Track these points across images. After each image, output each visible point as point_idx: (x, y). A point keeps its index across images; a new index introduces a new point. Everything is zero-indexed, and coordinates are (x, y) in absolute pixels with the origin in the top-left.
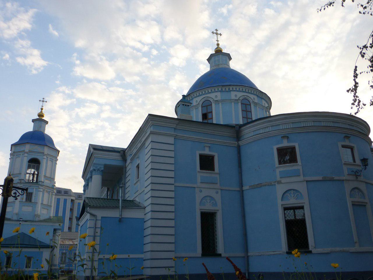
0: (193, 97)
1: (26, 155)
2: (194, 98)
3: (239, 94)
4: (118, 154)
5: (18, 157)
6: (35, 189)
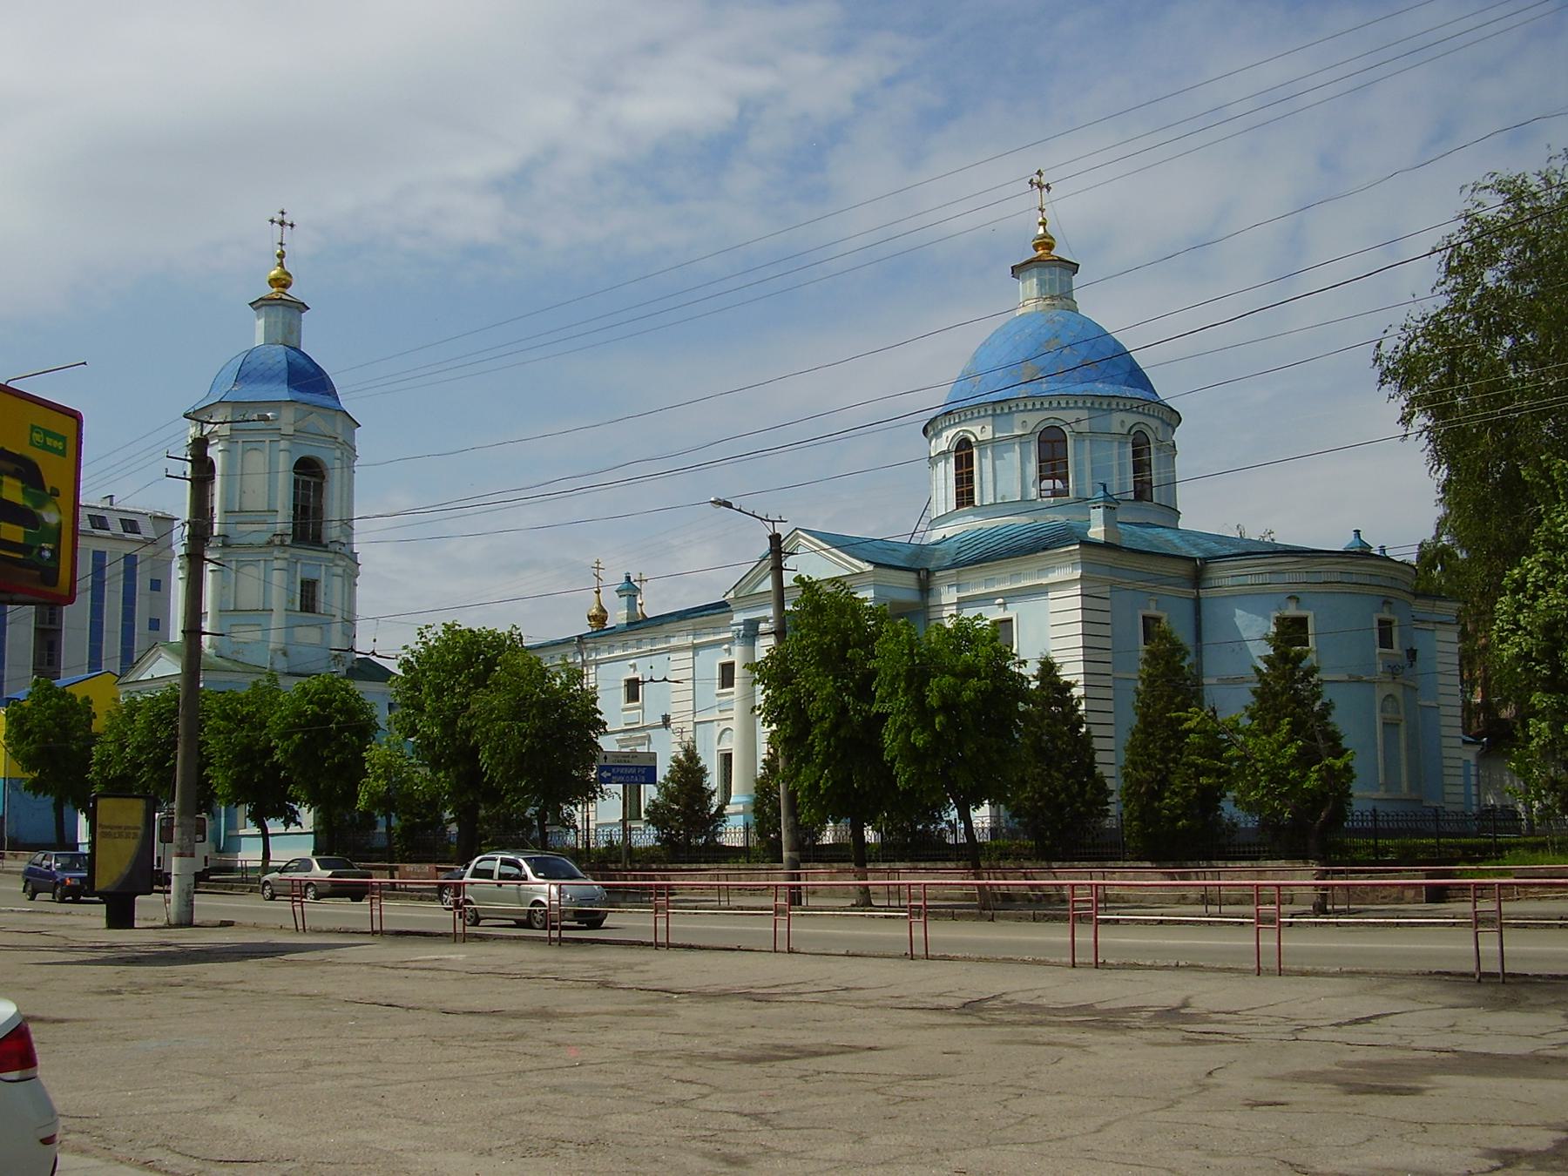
0: (1014, 409)
1: (283, 444)
2: (1016, 412)
3: (1130, 419)
4: (913, 576)
5: (251, 449)
6: (323, 567)
